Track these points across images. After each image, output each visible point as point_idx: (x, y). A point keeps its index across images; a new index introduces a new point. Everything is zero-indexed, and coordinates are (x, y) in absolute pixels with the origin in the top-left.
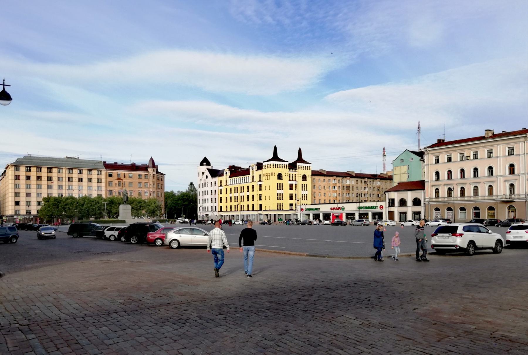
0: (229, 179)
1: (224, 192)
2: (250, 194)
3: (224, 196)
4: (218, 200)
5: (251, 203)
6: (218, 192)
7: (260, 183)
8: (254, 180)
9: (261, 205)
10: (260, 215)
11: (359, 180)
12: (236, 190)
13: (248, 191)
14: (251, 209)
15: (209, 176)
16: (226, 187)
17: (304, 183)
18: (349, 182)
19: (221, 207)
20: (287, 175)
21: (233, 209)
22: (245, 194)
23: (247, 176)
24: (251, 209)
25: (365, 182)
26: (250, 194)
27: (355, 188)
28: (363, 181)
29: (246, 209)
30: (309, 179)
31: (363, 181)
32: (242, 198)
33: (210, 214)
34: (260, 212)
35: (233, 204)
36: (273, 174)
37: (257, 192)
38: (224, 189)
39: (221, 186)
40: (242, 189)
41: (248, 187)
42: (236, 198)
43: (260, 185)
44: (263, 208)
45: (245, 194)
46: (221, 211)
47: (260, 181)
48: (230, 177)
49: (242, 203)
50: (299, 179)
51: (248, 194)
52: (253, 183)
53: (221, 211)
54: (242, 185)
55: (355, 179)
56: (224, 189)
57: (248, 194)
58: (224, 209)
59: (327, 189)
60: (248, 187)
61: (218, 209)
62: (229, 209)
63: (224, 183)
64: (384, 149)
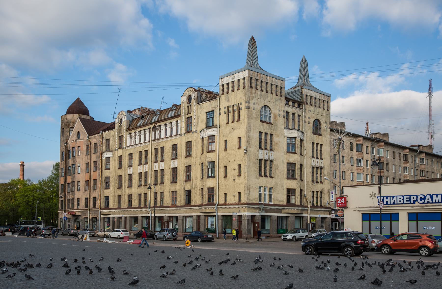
2: (180, 164)
7: (211, 132)
10: (208, 215)
11: (397, 151)
12: (143, 157)
15: (83, 131)
16: (120, 152)
17: (317, 139)
18: (382, 153)
19: (107, 198)
21: (135, 203)
22: (166, 166)
25: (406, 156)
26: (180, 164)
27: (390, 166)
28: (402, 155)
31: (402, 155)
34: (209, 209)
41: (175, 147)
42: (143, 176)
44: (218, 198)
45: (166, 166)
48: (128, 130)
51: (175, 164)
52: (189, 137)
53: (107, 206)
55: (391, 149)
57: (175, 164)
58: (113, 203)
60: (175, 147)
62: (125, 204)
63: (115, 143)
64: (367, 124)
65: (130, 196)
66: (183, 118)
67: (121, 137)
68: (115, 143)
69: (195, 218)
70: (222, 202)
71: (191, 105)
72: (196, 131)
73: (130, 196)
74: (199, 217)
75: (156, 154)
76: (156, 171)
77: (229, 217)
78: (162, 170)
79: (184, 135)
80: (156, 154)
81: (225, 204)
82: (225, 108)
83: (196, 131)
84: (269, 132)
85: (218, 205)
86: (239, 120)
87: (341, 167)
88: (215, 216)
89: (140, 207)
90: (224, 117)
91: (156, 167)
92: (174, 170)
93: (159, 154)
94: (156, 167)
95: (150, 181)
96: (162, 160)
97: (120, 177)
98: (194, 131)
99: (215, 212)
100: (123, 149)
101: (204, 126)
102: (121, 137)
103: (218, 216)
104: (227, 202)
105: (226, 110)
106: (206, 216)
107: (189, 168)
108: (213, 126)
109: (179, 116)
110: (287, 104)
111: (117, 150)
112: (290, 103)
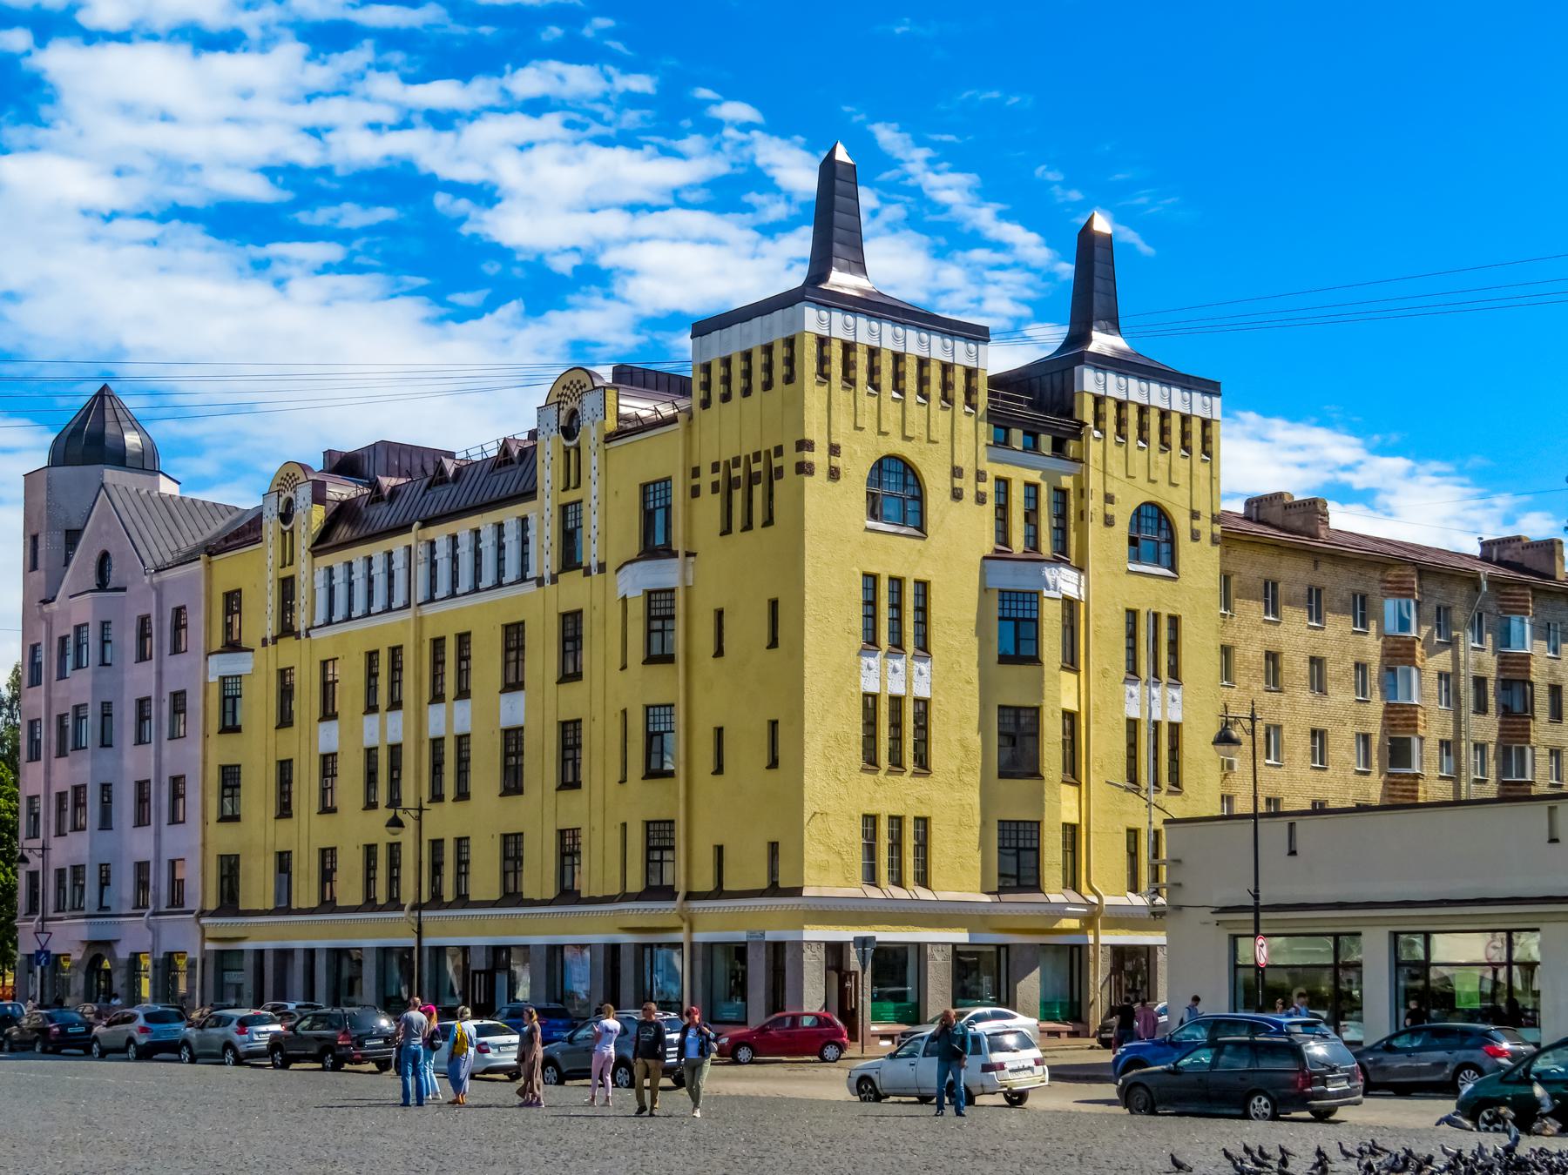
0: (309, 573)
1: (258, 706)
3: (257, 749)
4: (201, 797)
5: (539, 814)
6: (204, 708)
8: (590, 553)
9: (659, 838)
12: (383, 678)
13: (513, 685)
14: (539, 877)
16: (289, 653)
20: (968, 485)
21: (349, 889)
23: (509, 516)
24: (539, 877)
29: (485, 879)
30: (1201, 562)
32: (449, 765)
33: (134, 937)
35: (357, 828)
36: (819, 457)
37: (615, 688)
38: (254, 672)
39: (233, 646)
40: (449, 666)
41: (514, 636)
42: (381, 769)
43: (659, 608)
46: (229, 902)
47: (654, 548)
49: (445, 821)
50: (1106, 544)
51: (513, 709)
52: (574, 591)
53: (229, 902)
54: (446, 617)
56: (254, 672)
57: (513, 709)
58: (258, 887)
59: (1341, 695)
61: (201, 888)
62: (306, 891)
63: (260, 619)
65: (328, 857)
66: (548, 503)
67: (287, 587)
68: (260, 619)
69: (541, 959)
70: (705, 882)
71: (578, 449)
72: (602, 568)
73: (328, 857)
74: (614, 950)
75: (438, 662)
76: (437, 743)
77: (739, 952)
78: (462, 740)
79: (554, 579)
80: (438, 662)
81: (719, 893)
82: (715, 467)
83: (602, 568)
84: (911, 575)
85: (690, 896)
86: (769, 521)
87: (124, 912)
88: (680, 945)
89: (370, 904)
90: (710, 505)
91: (438, 721)
92: (513, 739)
93: (449, 666)
94: (438, 721)
95: (413, 788)
96: (463, 693)
97: (285, 767)
98: (594, 563)
99: (677, 929)
100: (298, 637)
101: (634, 547)
102: (287, 587)
103: (692, 945)
104: (725, 888)
105: (719, 477)
106: (644, 946)
107: (570, 734)
108: (668, 552)
109: (530, 494)
110: (1003, 442)
111: (275, 640)
112: (1017, 436)
